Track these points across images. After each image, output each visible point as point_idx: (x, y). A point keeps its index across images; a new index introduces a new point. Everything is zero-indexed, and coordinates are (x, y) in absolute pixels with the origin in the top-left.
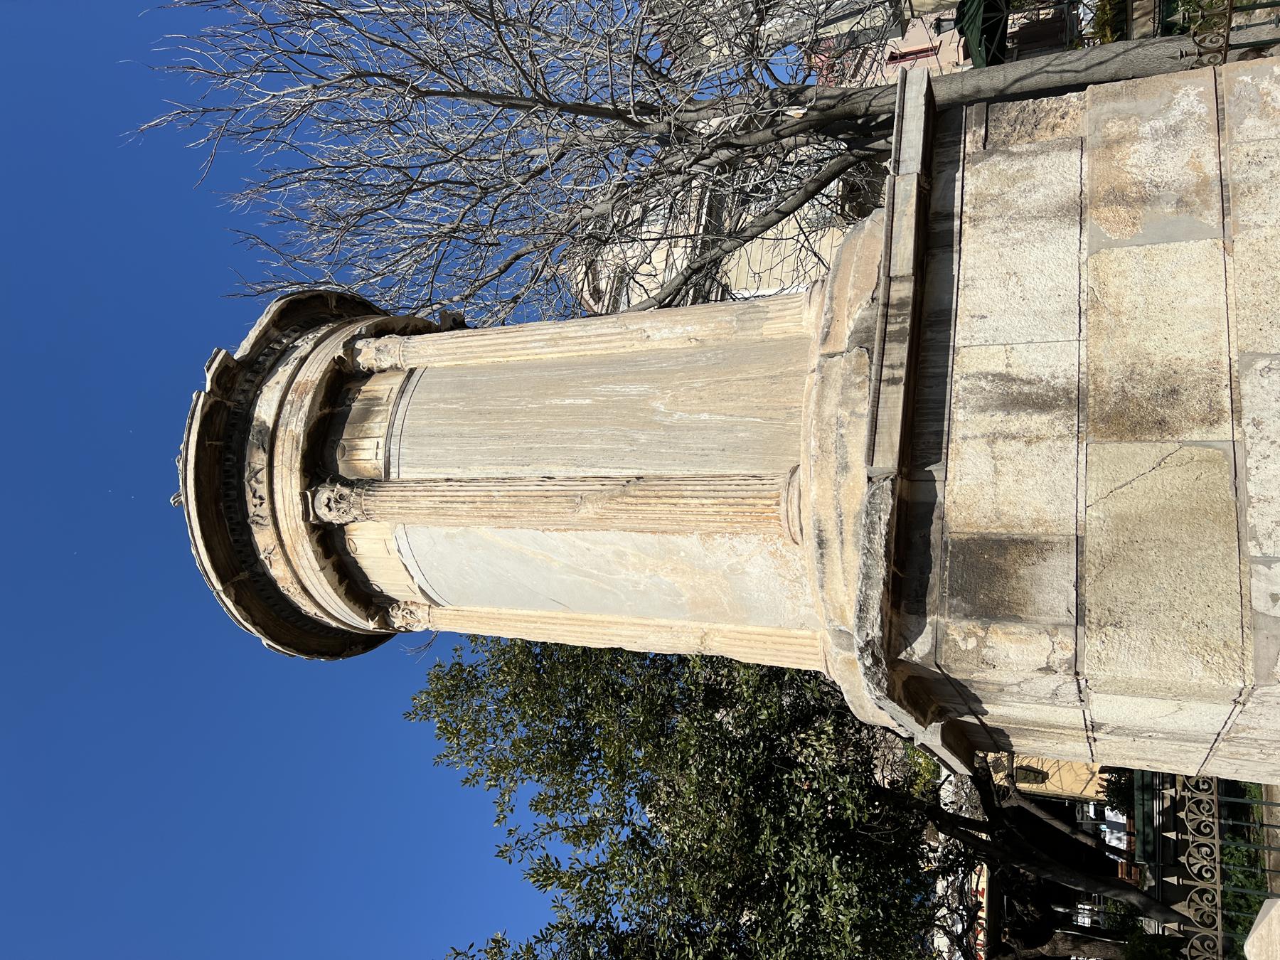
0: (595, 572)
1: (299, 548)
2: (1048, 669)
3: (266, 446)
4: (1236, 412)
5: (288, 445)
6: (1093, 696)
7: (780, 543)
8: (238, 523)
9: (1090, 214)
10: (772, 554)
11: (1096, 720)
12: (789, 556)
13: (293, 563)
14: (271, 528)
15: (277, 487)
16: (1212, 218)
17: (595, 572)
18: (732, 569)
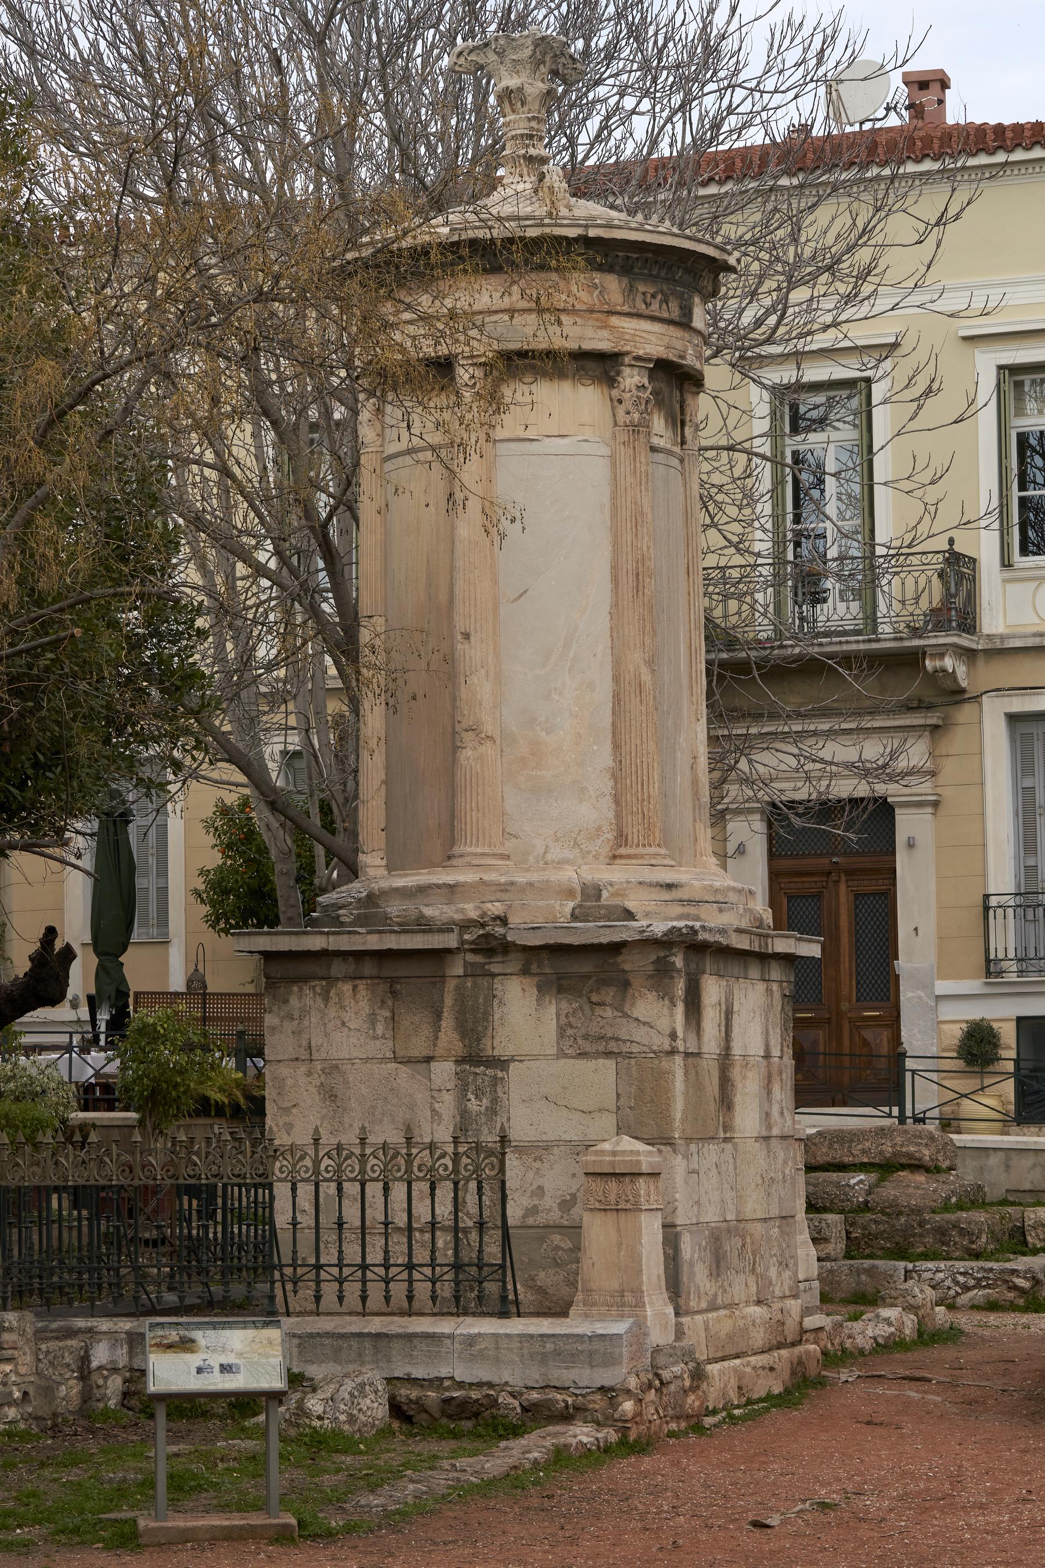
0: (571, 655)
1: (605, 333)
2: (673, 1036)
3: (683, 320)
4: (726, 1140)
5: (678, 345)
6: (611, 1063)
7: (610, 836)
8: (632, 268)
9: (764, 1062)
10: (600, 827)
11: (512, 1066)
12: (599, 842)
13: (587, 315)
14: (626, 309)
15: (657, 327)
16: (764, 1133)
17: (571, 655)
18: (583, 790)
